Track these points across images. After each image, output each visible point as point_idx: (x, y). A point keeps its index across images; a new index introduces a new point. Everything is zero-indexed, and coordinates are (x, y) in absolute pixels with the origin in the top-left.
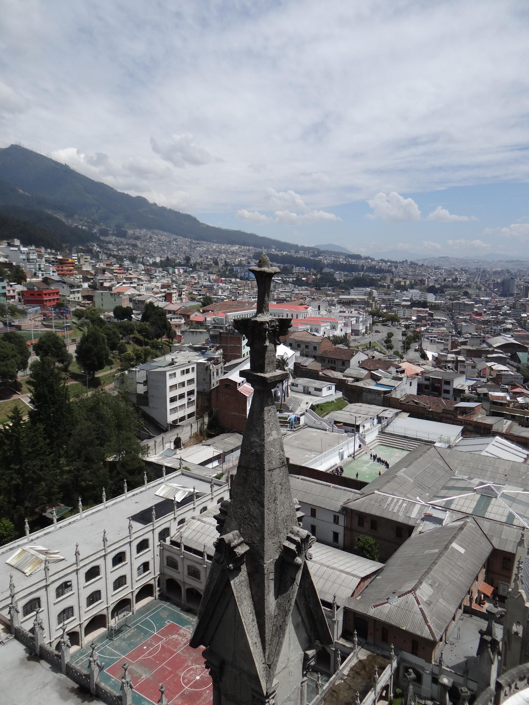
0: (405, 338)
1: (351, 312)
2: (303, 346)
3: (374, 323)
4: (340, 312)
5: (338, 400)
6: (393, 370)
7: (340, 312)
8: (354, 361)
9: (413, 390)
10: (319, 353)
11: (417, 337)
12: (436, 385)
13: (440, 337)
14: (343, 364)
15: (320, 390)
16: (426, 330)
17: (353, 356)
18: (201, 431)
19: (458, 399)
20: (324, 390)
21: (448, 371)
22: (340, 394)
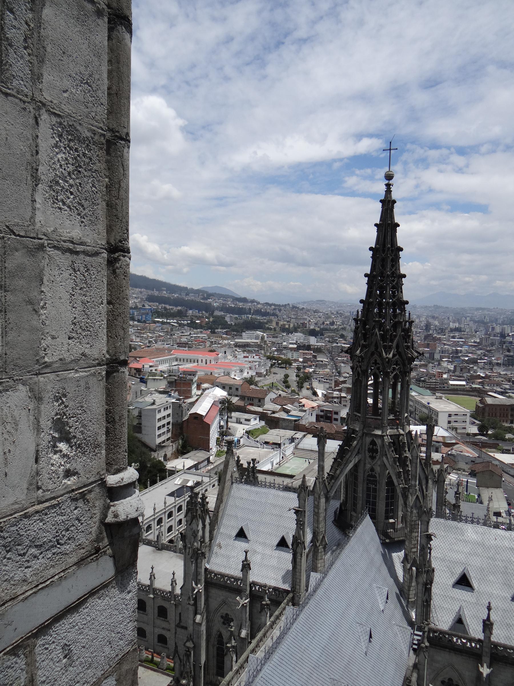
0: (298, 379)
1: (253, 357)
2: (227, 388)
3: (272, 366)
4: (245, 357)
5: (262, 427)
6: (296, 404)
7: (245, 357)
8: (267, 399)
9: (313, 419)
10: (239, 393)
11: (307, 378)
12: (329, 415)
13: (326, 378)
14: (259, 401)
15: (249, 420)
16: (314, 371)
17: (266, 395)
18: (177, 450)
19: (344, 424)
20: (252, 420)
21: (335, 405)
22: (263, 423)
